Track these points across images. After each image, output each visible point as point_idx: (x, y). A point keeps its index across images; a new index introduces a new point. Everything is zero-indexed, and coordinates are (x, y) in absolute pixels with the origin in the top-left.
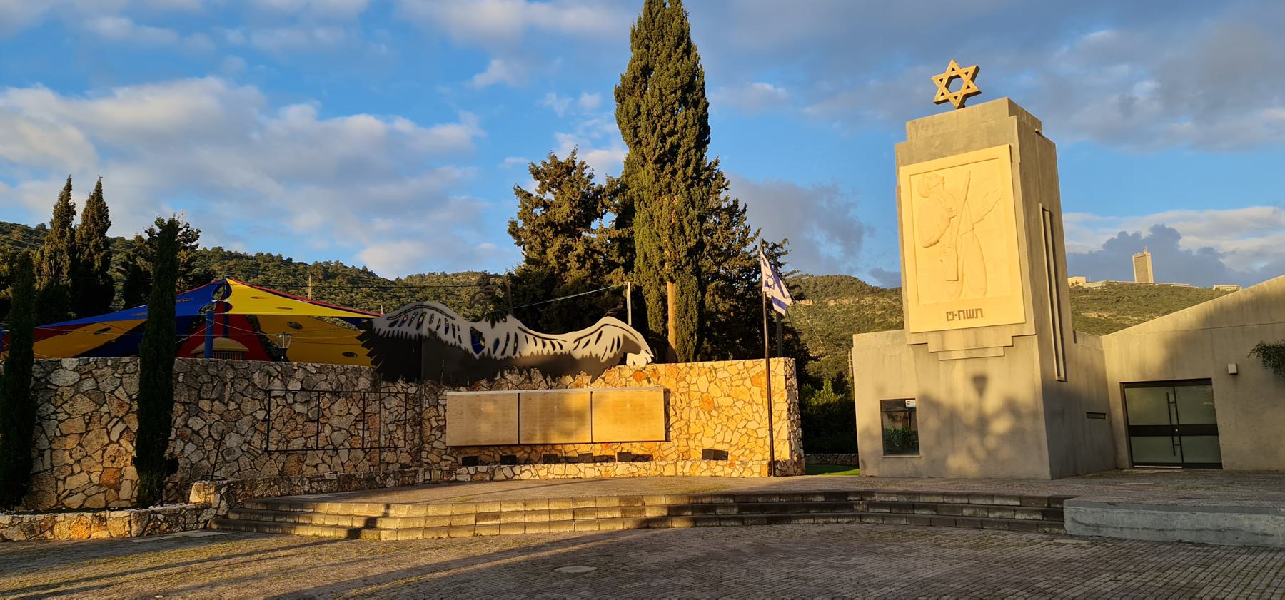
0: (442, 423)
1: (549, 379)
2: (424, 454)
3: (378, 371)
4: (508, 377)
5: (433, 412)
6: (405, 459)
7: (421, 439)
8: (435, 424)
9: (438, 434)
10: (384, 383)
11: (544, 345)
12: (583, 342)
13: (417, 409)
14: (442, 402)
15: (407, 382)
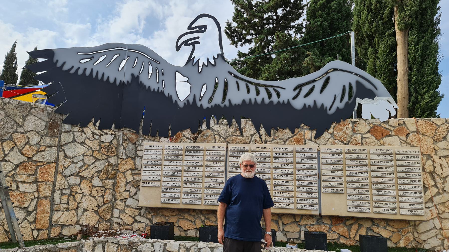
0: (137, 178)
1: (263, 131)
2: (116, 213)
3: (56, 112)
4: (216, 127)
5: (130, 164)
6: (90, 219)
7: (114, 195)
8: (130, 178)
9: (133, 190)
10: (67, 127)
11: (258, 93)
12: (305, 90)
13: (112, 160)
14: (139, 154)
15: (100, 128)
